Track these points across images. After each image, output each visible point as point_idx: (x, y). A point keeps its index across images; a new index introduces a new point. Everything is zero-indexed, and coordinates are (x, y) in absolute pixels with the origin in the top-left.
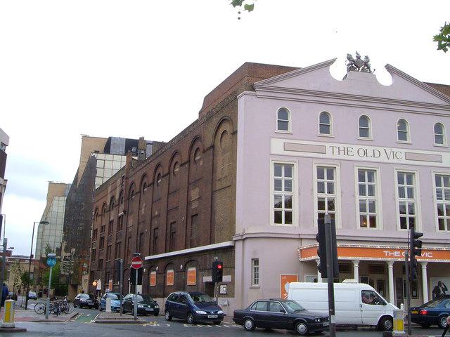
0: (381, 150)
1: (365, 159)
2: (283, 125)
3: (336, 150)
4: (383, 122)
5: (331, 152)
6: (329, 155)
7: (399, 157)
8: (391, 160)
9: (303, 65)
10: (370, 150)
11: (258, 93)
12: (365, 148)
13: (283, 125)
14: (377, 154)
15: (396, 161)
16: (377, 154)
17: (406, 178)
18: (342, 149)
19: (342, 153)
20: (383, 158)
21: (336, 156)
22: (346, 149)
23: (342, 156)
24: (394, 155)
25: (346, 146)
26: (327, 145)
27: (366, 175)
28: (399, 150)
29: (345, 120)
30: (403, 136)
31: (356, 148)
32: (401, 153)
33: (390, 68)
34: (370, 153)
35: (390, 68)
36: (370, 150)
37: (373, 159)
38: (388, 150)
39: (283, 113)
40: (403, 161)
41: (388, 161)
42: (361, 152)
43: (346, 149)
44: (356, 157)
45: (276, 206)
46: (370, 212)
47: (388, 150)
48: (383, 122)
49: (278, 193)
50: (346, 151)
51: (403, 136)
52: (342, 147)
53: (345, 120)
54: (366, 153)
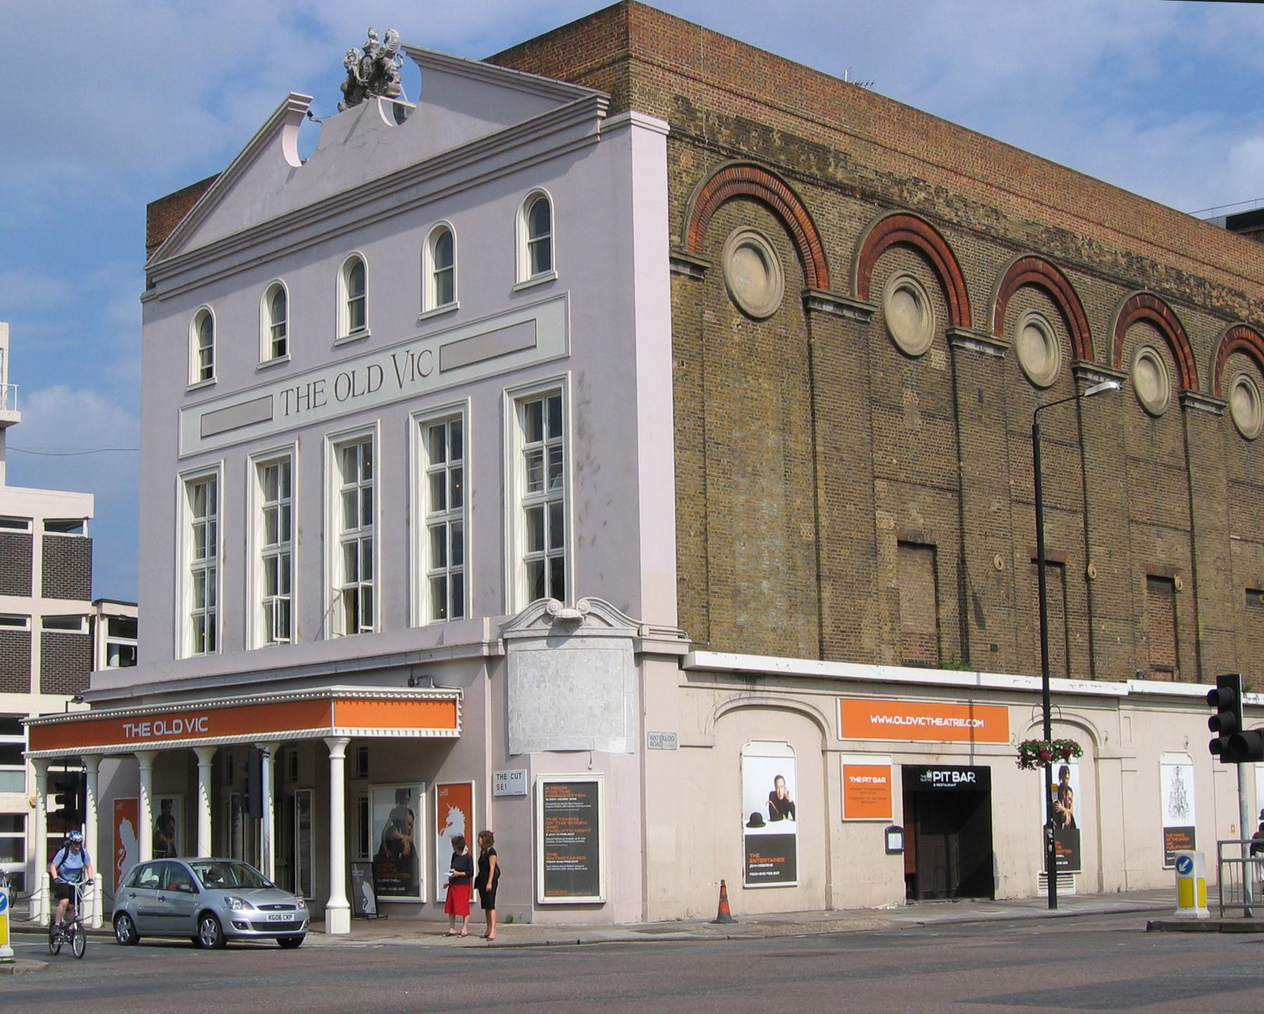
0: (385, 360)
8: (409, 390)
11: (159, 289)
12: (348, 368)
15: (421, 386)
17: (446, 436)
18: (303, 392)
19: (303, 402)
21: (295, 421)
26: (275, 390)
31: (330, 375)
32: (430, 352)
36: (360, 367)
44: (334, 409)
50: (311, 398)
52: (302, 383)
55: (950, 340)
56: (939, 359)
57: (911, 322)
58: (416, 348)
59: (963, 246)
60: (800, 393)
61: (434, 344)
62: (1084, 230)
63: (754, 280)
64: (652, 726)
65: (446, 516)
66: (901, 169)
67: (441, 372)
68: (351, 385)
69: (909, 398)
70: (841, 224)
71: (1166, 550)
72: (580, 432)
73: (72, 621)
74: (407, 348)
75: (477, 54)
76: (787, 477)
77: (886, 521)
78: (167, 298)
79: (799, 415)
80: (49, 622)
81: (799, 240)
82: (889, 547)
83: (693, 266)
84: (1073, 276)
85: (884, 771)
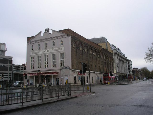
4: (50, 43)
8: (51, 52)
9: (35, 35)
20: (49, 52)
21: (41, 53)
24: (51, 50)
27: (46, 56)
30: (54, 45)
32: (53, 49)
33: (51, 30)
34: (47, 51)
35: (51, 30)
36: (47, 50)
37: (47, 52)
40: (53, 51)
44: (44, 53)
48: (50, 43)
50: (42, 52)
51: (54, 45)
52: (42, 51)
53: (43, 44)
55: (82, 50)
56: (82, 51)
57: (81, 49)
59: (83, 44)
60: (76, 53)
62: (88, 43)
63: (74, 46)
64: (71, 74)
66: (80, 39)
69: (81, 54)
70: (78, 42)
71: (92, 63)
72: (65, 55)
73: (11, 66)
75: (57, 30)
76: (76, 59)
77: (80, 61)
78: (29, 44)
79: (76, 55)
80: (9, 66)
81: (76, 43)
82: (80, 63)
83: (72, 45)
84: (88, 46)
85: (80, 77)
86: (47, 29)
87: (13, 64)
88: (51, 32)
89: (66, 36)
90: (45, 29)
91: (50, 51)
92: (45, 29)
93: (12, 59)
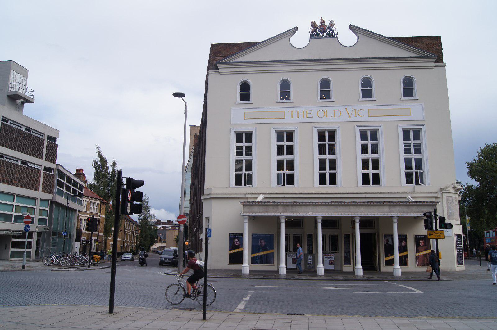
0: (343, 110)
1: (325, 119)
2: (245, 97)
3: (295, 114)
5: (289, 116)
6: (288, 119)
7: (365, 114)
8: (353, 119)
10: (330, 111)
11: (220, 70)
12: (324, 109)
13: (245, 97)
14: (337, 113)
15: (358, 119)
16: (337, 113)
21: (295, 120)
22: (305, 112)
23: (301, 120)
25: (305, 109)
26: (286, 110)
28: (362, 108)
29: (305, 84)
31: (315, 110)
33: (352, 27)
35: (352, 27)
36: (330, 111)
38: (350, 109)
39: (245, 86)
41: (349, 120)
42: (321, 114)
43: (305, 112)
45: (237, 170)
46: (373, 169)
47: (350, 109)
48: (346, 83)
49: (239, 158)
52: (301, 111)
53: (305, 84)
54: (325, 113)
58: (357, 108)
61: (366, 109)
65: (413, 156)
67: (369, 116)
68: (325, 113)
74: (353, 107)
86: (323, 22)
87: (57, 163)
88: (347, 39)
89: (433, 64)
90: (313, 24)
91: (347, 115)
92: (313, 24)
93: (57, 142)
